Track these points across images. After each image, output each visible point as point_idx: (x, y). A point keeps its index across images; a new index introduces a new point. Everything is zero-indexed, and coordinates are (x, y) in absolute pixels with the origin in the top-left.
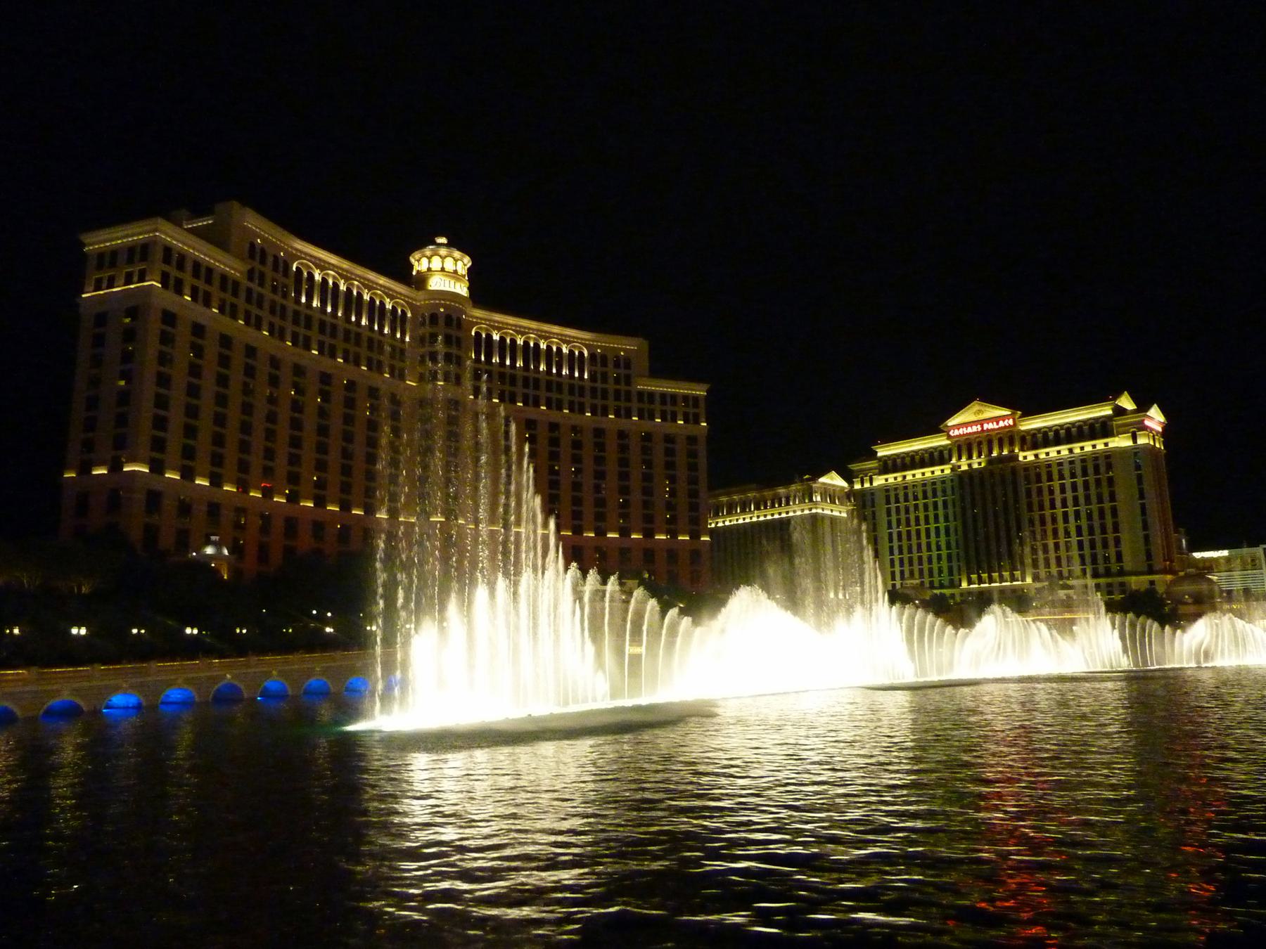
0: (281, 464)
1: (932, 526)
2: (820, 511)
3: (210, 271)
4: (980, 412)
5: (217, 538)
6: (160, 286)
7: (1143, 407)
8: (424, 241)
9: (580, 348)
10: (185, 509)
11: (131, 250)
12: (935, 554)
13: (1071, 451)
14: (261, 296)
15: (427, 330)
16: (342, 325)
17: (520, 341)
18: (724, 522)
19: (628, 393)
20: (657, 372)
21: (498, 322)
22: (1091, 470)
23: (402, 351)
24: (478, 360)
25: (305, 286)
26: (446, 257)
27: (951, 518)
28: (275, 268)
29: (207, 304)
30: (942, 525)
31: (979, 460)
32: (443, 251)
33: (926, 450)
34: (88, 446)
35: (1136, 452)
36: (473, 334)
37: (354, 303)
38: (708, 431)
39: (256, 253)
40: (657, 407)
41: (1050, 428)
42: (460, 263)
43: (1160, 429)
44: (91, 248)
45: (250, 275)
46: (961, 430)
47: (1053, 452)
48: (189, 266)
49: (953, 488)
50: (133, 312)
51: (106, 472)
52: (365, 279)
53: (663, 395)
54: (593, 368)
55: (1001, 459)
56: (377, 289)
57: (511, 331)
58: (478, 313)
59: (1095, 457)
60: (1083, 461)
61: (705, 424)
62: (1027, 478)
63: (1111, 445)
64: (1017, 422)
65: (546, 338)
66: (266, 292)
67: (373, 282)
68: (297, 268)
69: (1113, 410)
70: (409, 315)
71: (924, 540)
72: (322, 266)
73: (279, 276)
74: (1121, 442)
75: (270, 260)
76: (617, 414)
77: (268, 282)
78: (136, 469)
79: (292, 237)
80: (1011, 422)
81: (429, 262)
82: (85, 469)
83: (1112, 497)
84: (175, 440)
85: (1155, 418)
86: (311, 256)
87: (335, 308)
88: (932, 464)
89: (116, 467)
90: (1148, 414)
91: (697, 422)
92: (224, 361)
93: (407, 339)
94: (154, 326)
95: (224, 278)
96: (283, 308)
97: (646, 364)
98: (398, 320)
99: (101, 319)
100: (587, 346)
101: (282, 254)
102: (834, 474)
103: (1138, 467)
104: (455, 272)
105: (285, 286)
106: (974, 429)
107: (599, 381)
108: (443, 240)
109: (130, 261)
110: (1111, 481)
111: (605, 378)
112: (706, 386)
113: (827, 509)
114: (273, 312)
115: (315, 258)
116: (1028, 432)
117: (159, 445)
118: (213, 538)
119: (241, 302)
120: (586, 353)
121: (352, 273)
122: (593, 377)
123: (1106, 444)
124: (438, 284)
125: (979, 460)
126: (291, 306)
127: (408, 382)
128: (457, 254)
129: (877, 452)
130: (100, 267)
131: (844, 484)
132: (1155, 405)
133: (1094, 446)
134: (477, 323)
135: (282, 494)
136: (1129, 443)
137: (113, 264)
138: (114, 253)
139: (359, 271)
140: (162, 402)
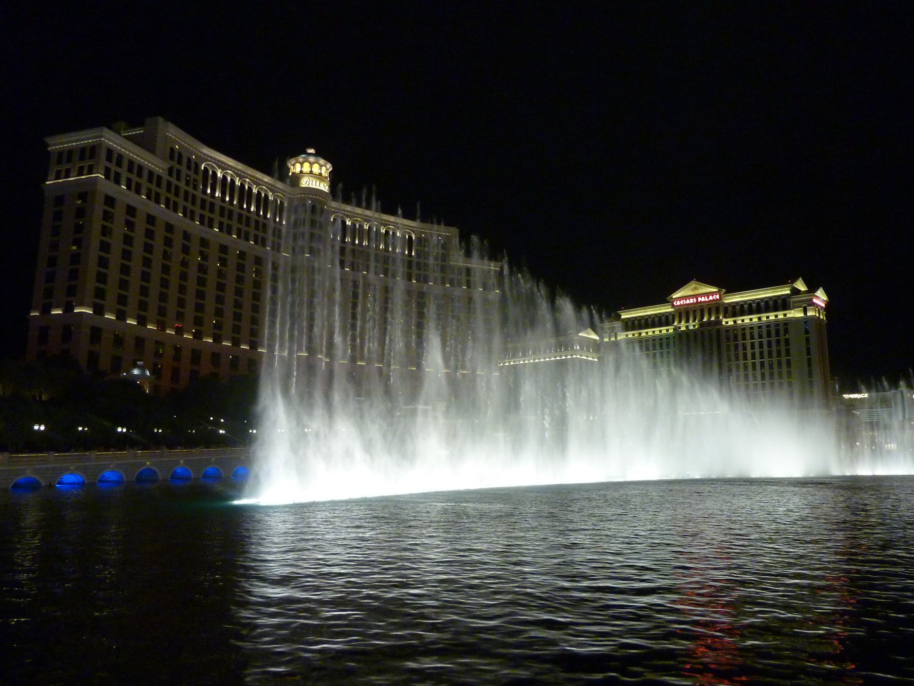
0: (190, 311)
2: (579, 357)
3: (140, 168)
4: (696, 288)
5: (142, 363)
6: (104, 177)
7: (812, 289)
8: (298, 151)
9: (409, 233)
10: (119, 341)
11: (83, 150)
13: (759, 319)
14: (177, 187)
16: (237, 210)
17: (366, 227)
18: (509, 363)
22: (773, 332)
25: (210, 182)
26: (314, 163)
28: (189, 168)
29: (138, 192)
31: (694, 323)
32: (312, 159)
33: (656, 315)
34: (49, 293)
35: (806, 321)
36: (332, 220)
37: (245, 194)
39: (173, 155)
41: (745, 302)
42: (324, 168)
43: (823, 305)
44: (53, 148)
45: (170, 171)
47: (747, 319)
48: (125, 164)
50: (83, 196)
51: (61, 313)
52: (254, 177)
55: (709, 323)
56: (264, 186)
57: (360, 219)
58: (334, 204)
59: (777, 323)
60: (768, 326)
62: (728, 339)
63: (788, 316)
64: (722, 297)
65: (385, 225)
66: (182, 185)
67: (260, 180)
68: (204, 168)
69: (791, 290)
70: (286, 205)
72: (224, 167)
73: (191, 173)
74: (796, 314)
75: (185, 160)
77: (183, 176)
78: (84, 311)
79: (203, 146)
80: (718, 297)
81: (302, 167)
82: (46, 310)
83: (788, 353)
84: (112, 291)
85: (821, 297)
86: (215, 159)
87: (232, 199)
88: (661, 325)
89: (68, 308)
90: (815, 294)
92: (150, 234)
94: (99, 207)
95: (151, 173)
96: (194, 196)
98: (279, 210)
99: (60, 200)
100: (413, 231)
101: (194, 157)
102: (590, 330)
103: (807, 332)
105: (195, 180)
106: (691, 301)
108: (312, 151)
109: (82, 158)
110: (787, 342)
113: (584, 356)
114: (186, 199)
115: (219, 161)
116: (729, 304)
117: (100, 294)
118: (139, 363)
119: (163, 191)
121: (244, 173)
123: (785, 315)
124: (308, 183)
125: (694, 323)
126: (199, 194)
128: (322, 161)
129: (621, 316)
130: (59, 162)
131: (597, 338)
132: (821, 288)
133: (776, 316)
135: (189, 332)
136: (802, 315)
137: (69, 160)
138: (70, 152)
139: (250, 171)
140: (103, 263)
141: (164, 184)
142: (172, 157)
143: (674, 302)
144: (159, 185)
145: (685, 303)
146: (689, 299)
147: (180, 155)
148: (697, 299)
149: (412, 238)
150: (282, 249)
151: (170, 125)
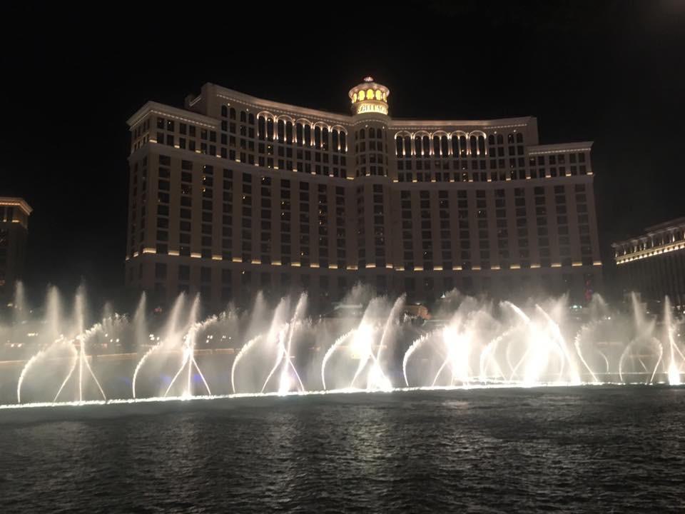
6: (156, 142)
8: (358, 81)
9: (480, 133)
15: (359, 142)
17: (431, 137)
19: (522, 162)
20: (546, 137)
21: (414, 127)
23: (343, 159)
24: (400, 155)
32: (365, 86)
36: (395, 138)
37: (305, 133)
38: (594, 177)
40: (547, 166)
42: (378, 93)
52: (310, 116)
54: (492, 146)
57: (424, 131)
61: (591, 173)
66: (238, 135)
70: (346, 134)
75: (238, 115)
76: (318, 172)
81: (358, 96)
91: (584, 172)
93: (346, 150)
104: (375, 98)
107: (497, 155)
108: (369, 79)
111: (501, 152)
112: (591, 143)
120: (485, 136)
126: (256, 141)
127: (348, 178)
134: (396, 131)
141: (219, 138)
142: (224, 114)
144: (213, 139)
147: (233, 111)
149: (483, 137)
150: (347, 174)
151: (217, 87)
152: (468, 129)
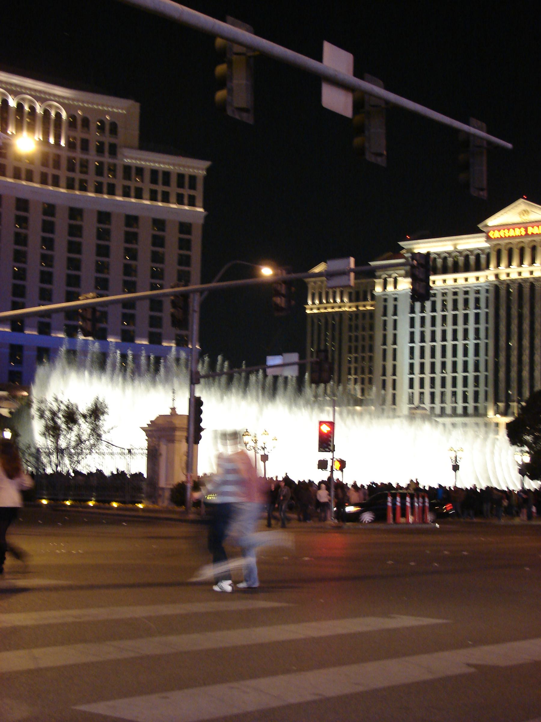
1: (460, 344)
4: (526, 212)
9: (57, 108)
12: (460, 375)
19: (113, 170)
27: (482, 334)
30: (471, 342)
38: (206, 218)
46: (502, 231)
49: (487, 299)
53: (154, 173)
54: (72, 134)
61: (201, 210)
71: (449, 360)
97: (136, 132)
106: (518, 232)
111: (85, 145)
112: (207, 164)
120: (64, 115)
122: (71, 145)
143: (489, 232)
145: (507, 236)
146: (514, 229)
148: (526, 230)
152: (42, 98)
